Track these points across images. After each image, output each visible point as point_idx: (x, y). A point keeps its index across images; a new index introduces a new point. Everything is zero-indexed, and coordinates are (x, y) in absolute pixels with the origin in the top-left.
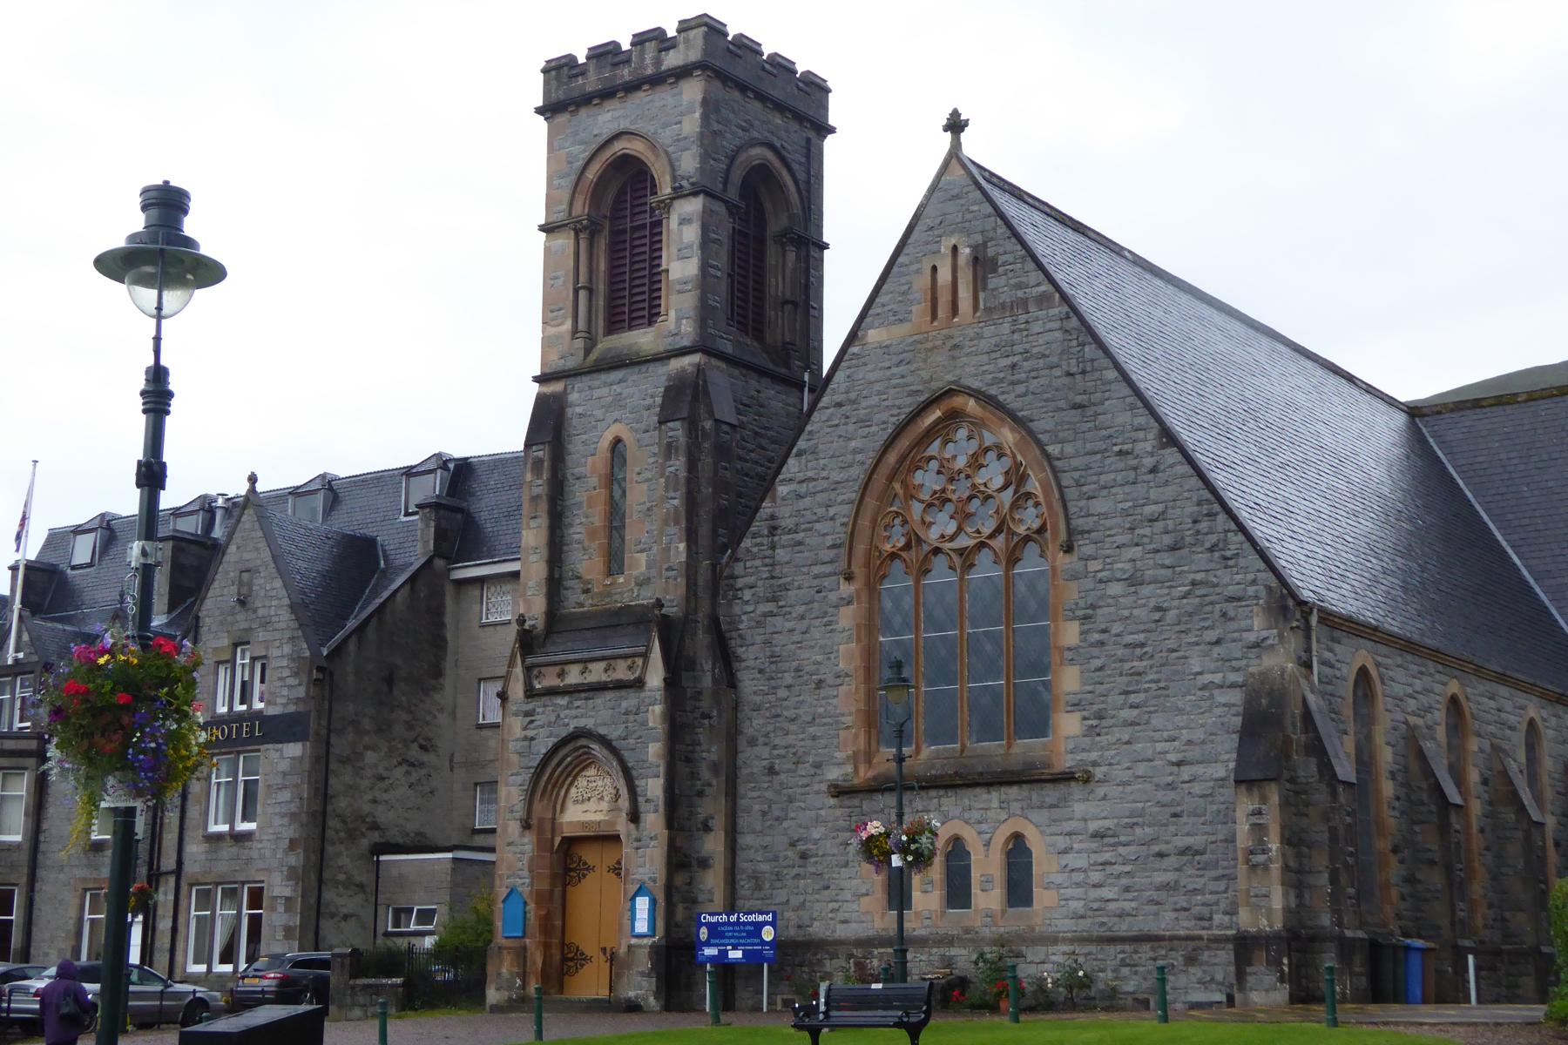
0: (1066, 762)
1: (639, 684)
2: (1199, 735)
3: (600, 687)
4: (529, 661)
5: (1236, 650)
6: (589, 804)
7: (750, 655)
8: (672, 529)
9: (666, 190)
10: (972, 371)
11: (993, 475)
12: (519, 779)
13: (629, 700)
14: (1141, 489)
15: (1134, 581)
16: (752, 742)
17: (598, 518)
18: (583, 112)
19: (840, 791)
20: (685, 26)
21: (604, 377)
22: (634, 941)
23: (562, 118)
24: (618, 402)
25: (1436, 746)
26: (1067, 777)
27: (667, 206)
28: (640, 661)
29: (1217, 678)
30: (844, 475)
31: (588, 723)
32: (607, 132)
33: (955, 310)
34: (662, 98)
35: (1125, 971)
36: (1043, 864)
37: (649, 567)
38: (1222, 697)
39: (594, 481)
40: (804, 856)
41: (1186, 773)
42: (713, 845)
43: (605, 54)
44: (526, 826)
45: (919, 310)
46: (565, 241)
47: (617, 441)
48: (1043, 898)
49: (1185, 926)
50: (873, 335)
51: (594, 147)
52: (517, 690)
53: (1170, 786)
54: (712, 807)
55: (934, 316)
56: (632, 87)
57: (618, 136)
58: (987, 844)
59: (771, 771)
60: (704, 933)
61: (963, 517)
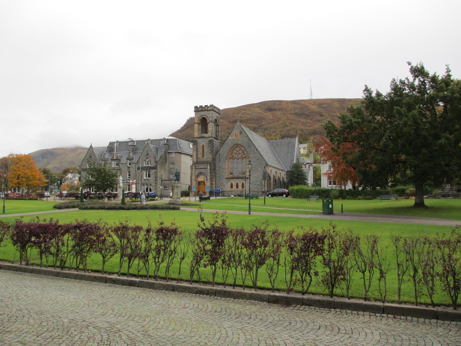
1: (207, 168)
6: (201, 179)
7: (217, 166)
9: (208, 121)
10: (239, 142)
11: (241, 152)
13: (206, 170)
17: (201, 152)
19: (227, 178)
20: (210, 106)
24: (203, 141)
25: (275, 175)
34: (208, 112)
42: (214, 183)
43: (201, 107)
45: (235, 136)
47: (203, 145)
49: (257, 190)
52: (194, 168)
56: (205, 111)
61: (238, 155)
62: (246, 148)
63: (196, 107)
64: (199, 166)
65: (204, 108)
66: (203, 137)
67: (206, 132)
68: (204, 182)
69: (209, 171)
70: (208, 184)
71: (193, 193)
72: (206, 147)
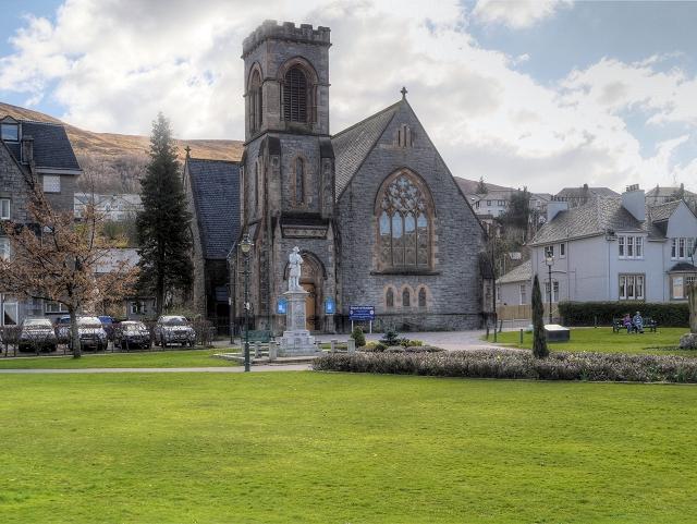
0: (437, 271)
1: (325, 238)
3: (314, 238)
7: (345, 232)
11: (412, 191)
15: (452, 227)
16: (345, 258)
17: (293, 181)
19: (376, 274)
26: (438, 274)
30: (372, 185)
36: (429, 295)
38: (472, 258)
39: (291, 170)
42: (339, 287)
48: (429, 304)
50: (382, 146)
57: (296, 57)
60: (352, 313)
61: (403, 202)
62: (428, 182)
65: (296, 31)
66: (299, 132)
69: (331, 248)
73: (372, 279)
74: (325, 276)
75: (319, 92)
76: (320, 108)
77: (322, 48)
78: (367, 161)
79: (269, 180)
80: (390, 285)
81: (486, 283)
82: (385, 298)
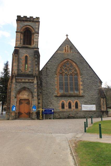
0: (81, 95)
1: (33, 83)
2: (95, 93)
3: (28, 82)
4: (16, 78)
5: (97, 86)
6: (25, 95)
7: (44, 81)
8: (36, 66)
10: (70, 57)
12: (15, 92)
14: (88, 71)
16: (44, 91)
18: (22, 22)
19: (56, 96)
20: (37, 18)
21: (26, 49)
22: (33, 112)
23: (19, 22)
26: (82, 96)
27: (34, 34)
28: (33, 80)
29: (96, 88)
31: (26, 86)
32: (27, 24)
33: (68, 52)
35: (89, 114)
37: (31, 70)
38: (97, 90)
40: (51, 103)
41: (94, 96)
42: (40, 101)
44: (16, 97)
45: (64, 51)
46: (19, 34)
51: (24, 25)
53: (92, 98)
54: (40, 97)
55: (66, 52)
56: (30, 21)
57: (28, 25)
58: (73, 102)
59: (47, 94)
62: (78, 63)
63: (19, 17)
64: (21, 80)
67: (30, 44)
68: (29, 100)
69: (36, 86)
70: (34, 102)
71: (13, 114)
72: (29, 59)
73: (56, 99)
74: (33, 97)
75: (35, 35)
76: (35, 40)
77: (37, 24)
78: (53, 57)
79: (14, 62)
80: (63, 101)
81: (102, 100)
82: (61, 105)
